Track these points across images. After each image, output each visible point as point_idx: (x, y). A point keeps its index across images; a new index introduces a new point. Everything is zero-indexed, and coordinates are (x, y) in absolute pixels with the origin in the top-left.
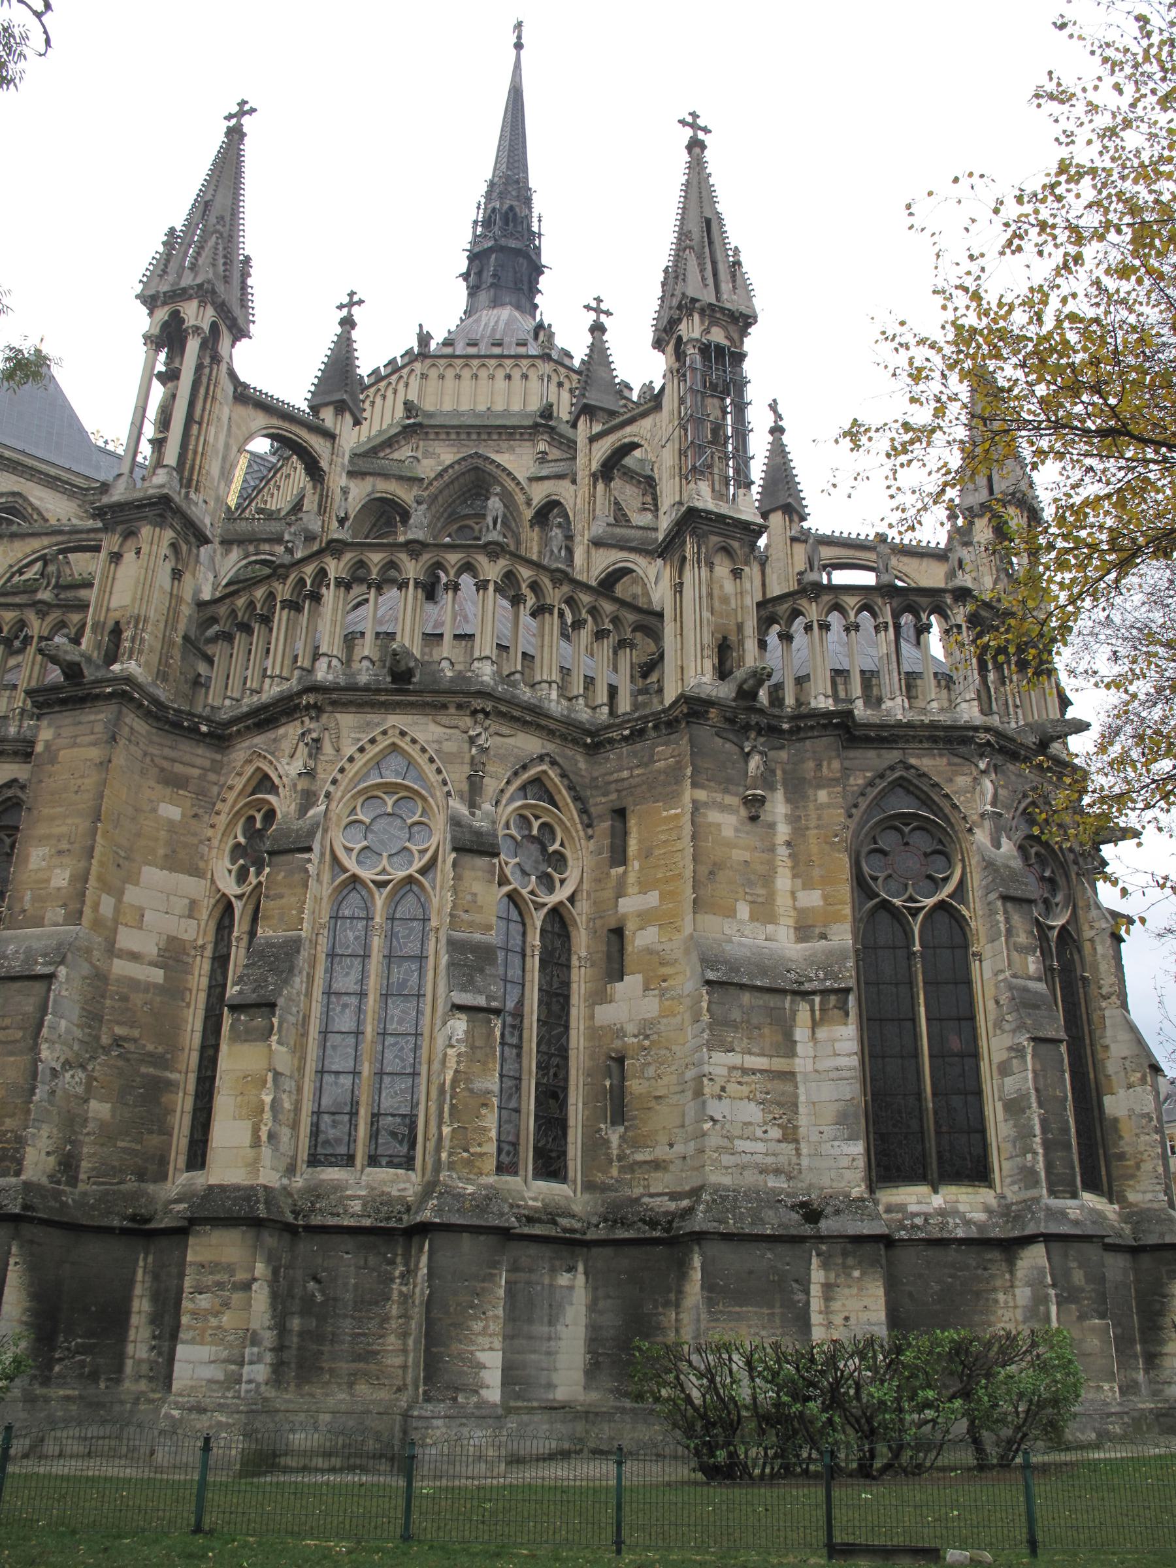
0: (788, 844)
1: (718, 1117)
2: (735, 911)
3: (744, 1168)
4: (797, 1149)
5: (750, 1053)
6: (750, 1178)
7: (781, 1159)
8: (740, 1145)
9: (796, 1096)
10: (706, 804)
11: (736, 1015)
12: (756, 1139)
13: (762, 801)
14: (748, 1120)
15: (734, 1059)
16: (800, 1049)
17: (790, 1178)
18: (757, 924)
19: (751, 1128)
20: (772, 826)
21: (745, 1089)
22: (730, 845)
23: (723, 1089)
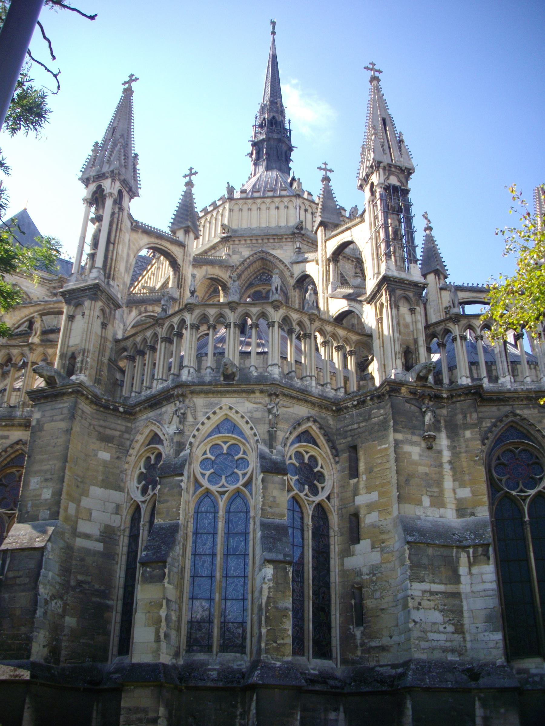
0: (450, 462)
1: (418, 620)
2: (421, 501)
3: (433, 649)
4: (464, 638)
5: (434, 583)
6: (437, 655)
7: (455, 643)
8: (431, 636)
9: (462, 607)
10: (402, 442)
11: (425, 561)
12: (440, 632)
13: (434, 438)
14: (434, 621)
16: (463, 579)
17: (460, 654)
18: (434, 508)
19: (437, 626)
20: (440, 452)
22: (416, 464)
23: (420, 604)
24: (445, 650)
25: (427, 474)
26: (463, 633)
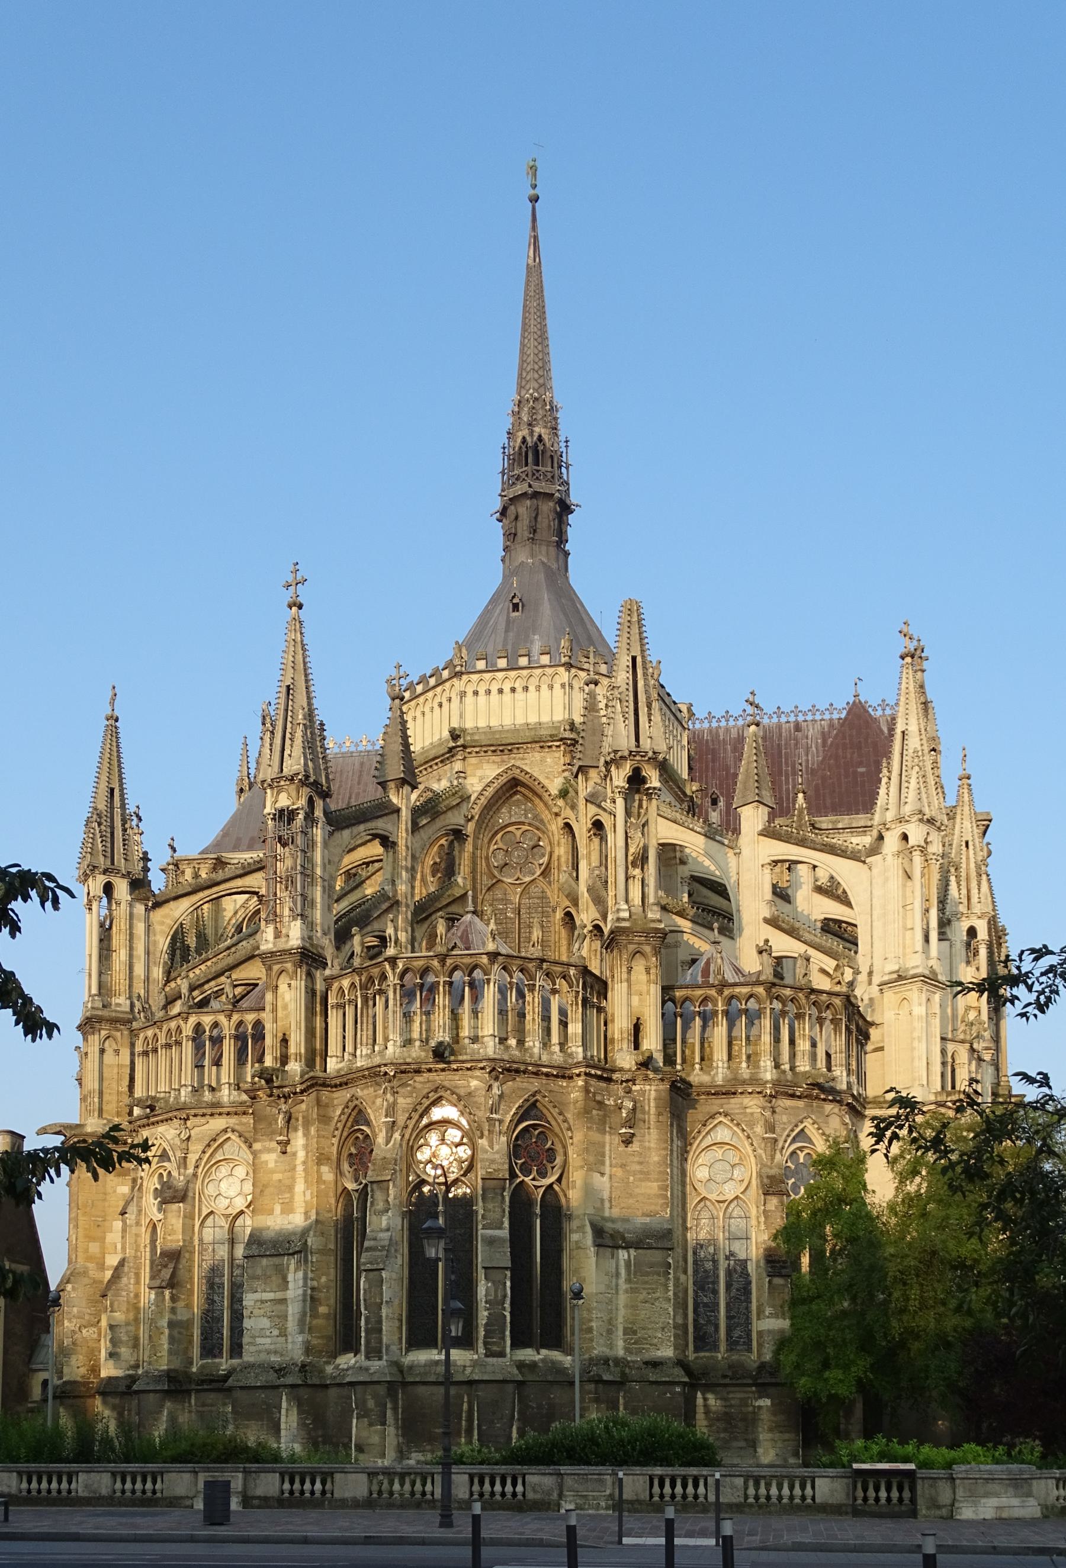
0: (304, 1163)
3: (260, 1352)
6: (263, 1357)
8: (259, 1340)
9: (287, 1311)
11: (259, 1272)
13: (288, 1142)
15: (257, 1296)
16: (291, 1285)
17: (282, 1355)
20: (294, 1154)
21: (262, 1311)
22: (273, 1172)
24: (269, 1352)
25: (280, 1181)
26: (286, 1336)
